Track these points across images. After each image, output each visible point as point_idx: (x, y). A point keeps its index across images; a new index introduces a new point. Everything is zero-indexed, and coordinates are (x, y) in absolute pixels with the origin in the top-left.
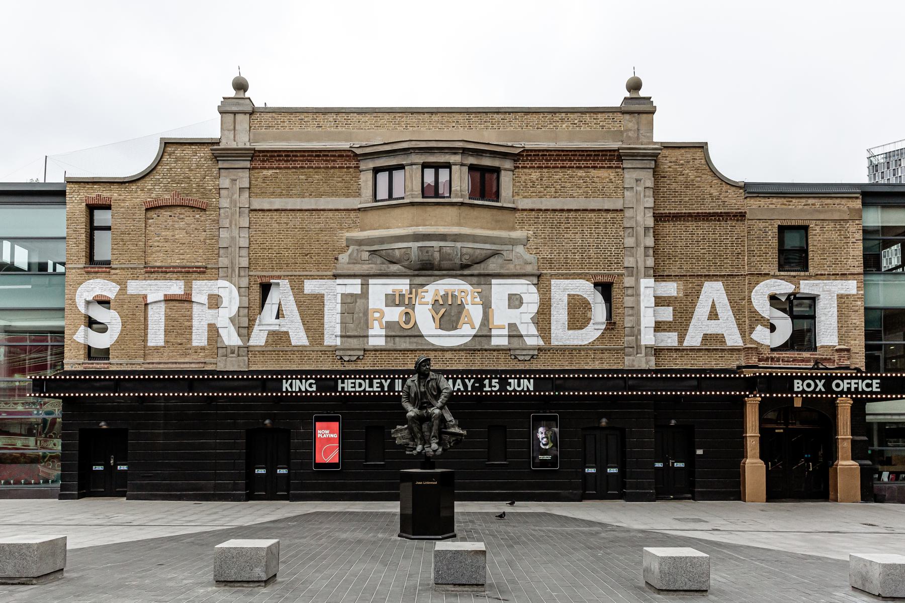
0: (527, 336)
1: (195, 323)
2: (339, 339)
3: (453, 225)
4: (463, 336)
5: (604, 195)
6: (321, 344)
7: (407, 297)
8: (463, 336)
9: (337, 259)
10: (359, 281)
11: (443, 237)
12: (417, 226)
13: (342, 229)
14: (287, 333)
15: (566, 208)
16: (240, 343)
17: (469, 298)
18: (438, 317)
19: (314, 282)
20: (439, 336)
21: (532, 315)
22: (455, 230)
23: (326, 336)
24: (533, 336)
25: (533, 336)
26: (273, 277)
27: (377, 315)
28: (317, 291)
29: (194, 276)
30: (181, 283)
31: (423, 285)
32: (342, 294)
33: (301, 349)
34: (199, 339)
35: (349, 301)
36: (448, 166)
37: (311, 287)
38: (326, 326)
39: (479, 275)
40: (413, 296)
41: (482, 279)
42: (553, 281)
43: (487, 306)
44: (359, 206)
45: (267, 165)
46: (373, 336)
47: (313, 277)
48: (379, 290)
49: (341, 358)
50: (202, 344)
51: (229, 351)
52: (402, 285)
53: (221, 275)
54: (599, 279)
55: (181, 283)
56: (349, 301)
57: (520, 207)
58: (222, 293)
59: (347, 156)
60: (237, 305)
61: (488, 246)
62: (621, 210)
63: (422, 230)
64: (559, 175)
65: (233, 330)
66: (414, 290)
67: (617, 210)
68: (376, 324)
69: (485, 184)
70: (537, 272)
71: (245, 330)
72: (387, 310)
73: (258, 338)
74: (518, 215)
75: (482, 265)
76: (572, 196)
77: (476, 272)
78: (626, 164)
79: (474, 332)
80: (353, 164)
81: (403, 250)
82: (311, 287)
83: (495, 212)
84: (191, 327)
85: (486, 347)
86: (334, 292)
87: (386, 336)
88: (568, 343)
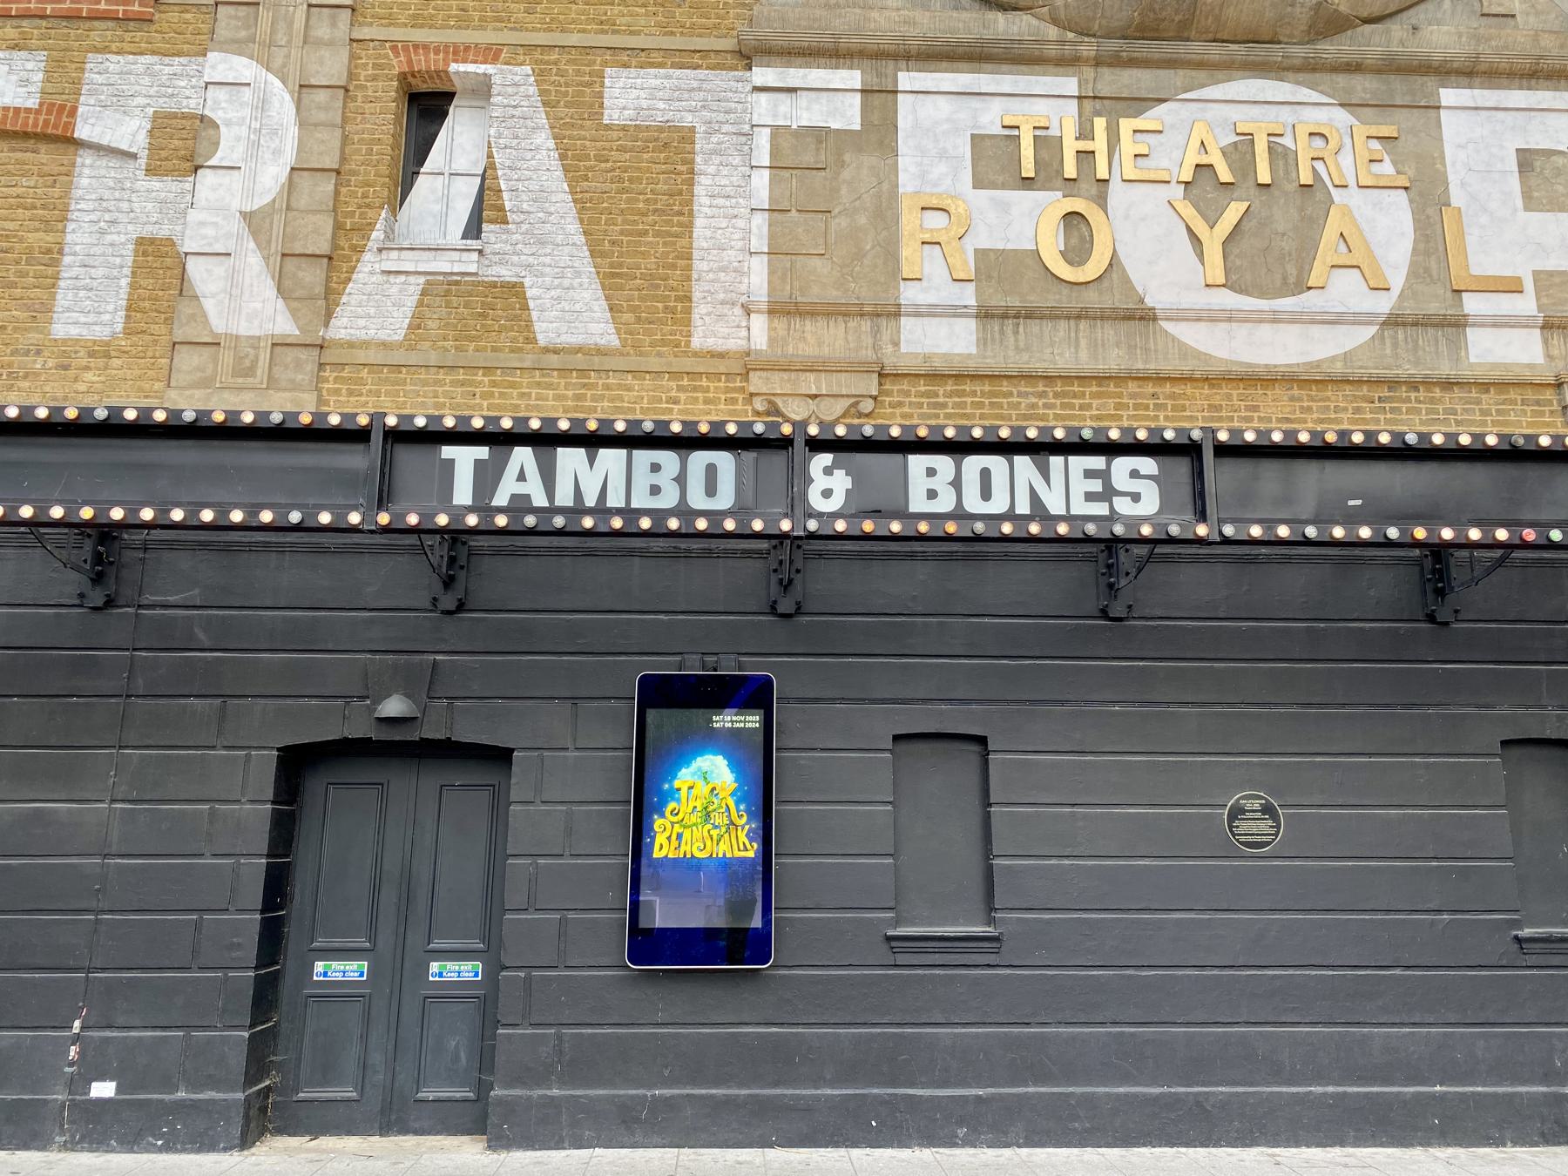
1: (78, 237)
2: (759, 323)
4: (1337, 320)
6: (680, 346)
7: (1070, 147)
8: (1337, 320)
10: (852, 77)
14: (515, 290)
16: (284, 325)
17: (1346, 160)
18: (1213, 242)
19: (653, 78)
20: (1230, 317)
23: (700, 310)
26: (462, 52)
27: (936, 221)
28: (662, 113)
29: (100, 32)
30: (33, 66)
31: (1138, 103)
32: (777, 132)
33: (579, 360)
34: (89, 303)
35: (808, 159)
37: (630, 95)
38: (699, 266)
39: (1393, 67)
40: (1100, 144)
41: (1399, 88)
43: (1428, 195)
46: (918, 313)
47: (642, 58)
48: (940, 116)
50: (101, 333)
51: (226, 357)
52: (1044, 104)
53: (222, 32)
55: (33, 66)
56: (804, 158)
58: (220, 107)
60: (289, 157)
65: (253, 262)
66: (1100, 123)
68: (933, 266)
71: (318, 268)
73: (376, 308)
79: (1383, 304)
82: (630, 95)
84: (53, 256)
85: (1445, 369)
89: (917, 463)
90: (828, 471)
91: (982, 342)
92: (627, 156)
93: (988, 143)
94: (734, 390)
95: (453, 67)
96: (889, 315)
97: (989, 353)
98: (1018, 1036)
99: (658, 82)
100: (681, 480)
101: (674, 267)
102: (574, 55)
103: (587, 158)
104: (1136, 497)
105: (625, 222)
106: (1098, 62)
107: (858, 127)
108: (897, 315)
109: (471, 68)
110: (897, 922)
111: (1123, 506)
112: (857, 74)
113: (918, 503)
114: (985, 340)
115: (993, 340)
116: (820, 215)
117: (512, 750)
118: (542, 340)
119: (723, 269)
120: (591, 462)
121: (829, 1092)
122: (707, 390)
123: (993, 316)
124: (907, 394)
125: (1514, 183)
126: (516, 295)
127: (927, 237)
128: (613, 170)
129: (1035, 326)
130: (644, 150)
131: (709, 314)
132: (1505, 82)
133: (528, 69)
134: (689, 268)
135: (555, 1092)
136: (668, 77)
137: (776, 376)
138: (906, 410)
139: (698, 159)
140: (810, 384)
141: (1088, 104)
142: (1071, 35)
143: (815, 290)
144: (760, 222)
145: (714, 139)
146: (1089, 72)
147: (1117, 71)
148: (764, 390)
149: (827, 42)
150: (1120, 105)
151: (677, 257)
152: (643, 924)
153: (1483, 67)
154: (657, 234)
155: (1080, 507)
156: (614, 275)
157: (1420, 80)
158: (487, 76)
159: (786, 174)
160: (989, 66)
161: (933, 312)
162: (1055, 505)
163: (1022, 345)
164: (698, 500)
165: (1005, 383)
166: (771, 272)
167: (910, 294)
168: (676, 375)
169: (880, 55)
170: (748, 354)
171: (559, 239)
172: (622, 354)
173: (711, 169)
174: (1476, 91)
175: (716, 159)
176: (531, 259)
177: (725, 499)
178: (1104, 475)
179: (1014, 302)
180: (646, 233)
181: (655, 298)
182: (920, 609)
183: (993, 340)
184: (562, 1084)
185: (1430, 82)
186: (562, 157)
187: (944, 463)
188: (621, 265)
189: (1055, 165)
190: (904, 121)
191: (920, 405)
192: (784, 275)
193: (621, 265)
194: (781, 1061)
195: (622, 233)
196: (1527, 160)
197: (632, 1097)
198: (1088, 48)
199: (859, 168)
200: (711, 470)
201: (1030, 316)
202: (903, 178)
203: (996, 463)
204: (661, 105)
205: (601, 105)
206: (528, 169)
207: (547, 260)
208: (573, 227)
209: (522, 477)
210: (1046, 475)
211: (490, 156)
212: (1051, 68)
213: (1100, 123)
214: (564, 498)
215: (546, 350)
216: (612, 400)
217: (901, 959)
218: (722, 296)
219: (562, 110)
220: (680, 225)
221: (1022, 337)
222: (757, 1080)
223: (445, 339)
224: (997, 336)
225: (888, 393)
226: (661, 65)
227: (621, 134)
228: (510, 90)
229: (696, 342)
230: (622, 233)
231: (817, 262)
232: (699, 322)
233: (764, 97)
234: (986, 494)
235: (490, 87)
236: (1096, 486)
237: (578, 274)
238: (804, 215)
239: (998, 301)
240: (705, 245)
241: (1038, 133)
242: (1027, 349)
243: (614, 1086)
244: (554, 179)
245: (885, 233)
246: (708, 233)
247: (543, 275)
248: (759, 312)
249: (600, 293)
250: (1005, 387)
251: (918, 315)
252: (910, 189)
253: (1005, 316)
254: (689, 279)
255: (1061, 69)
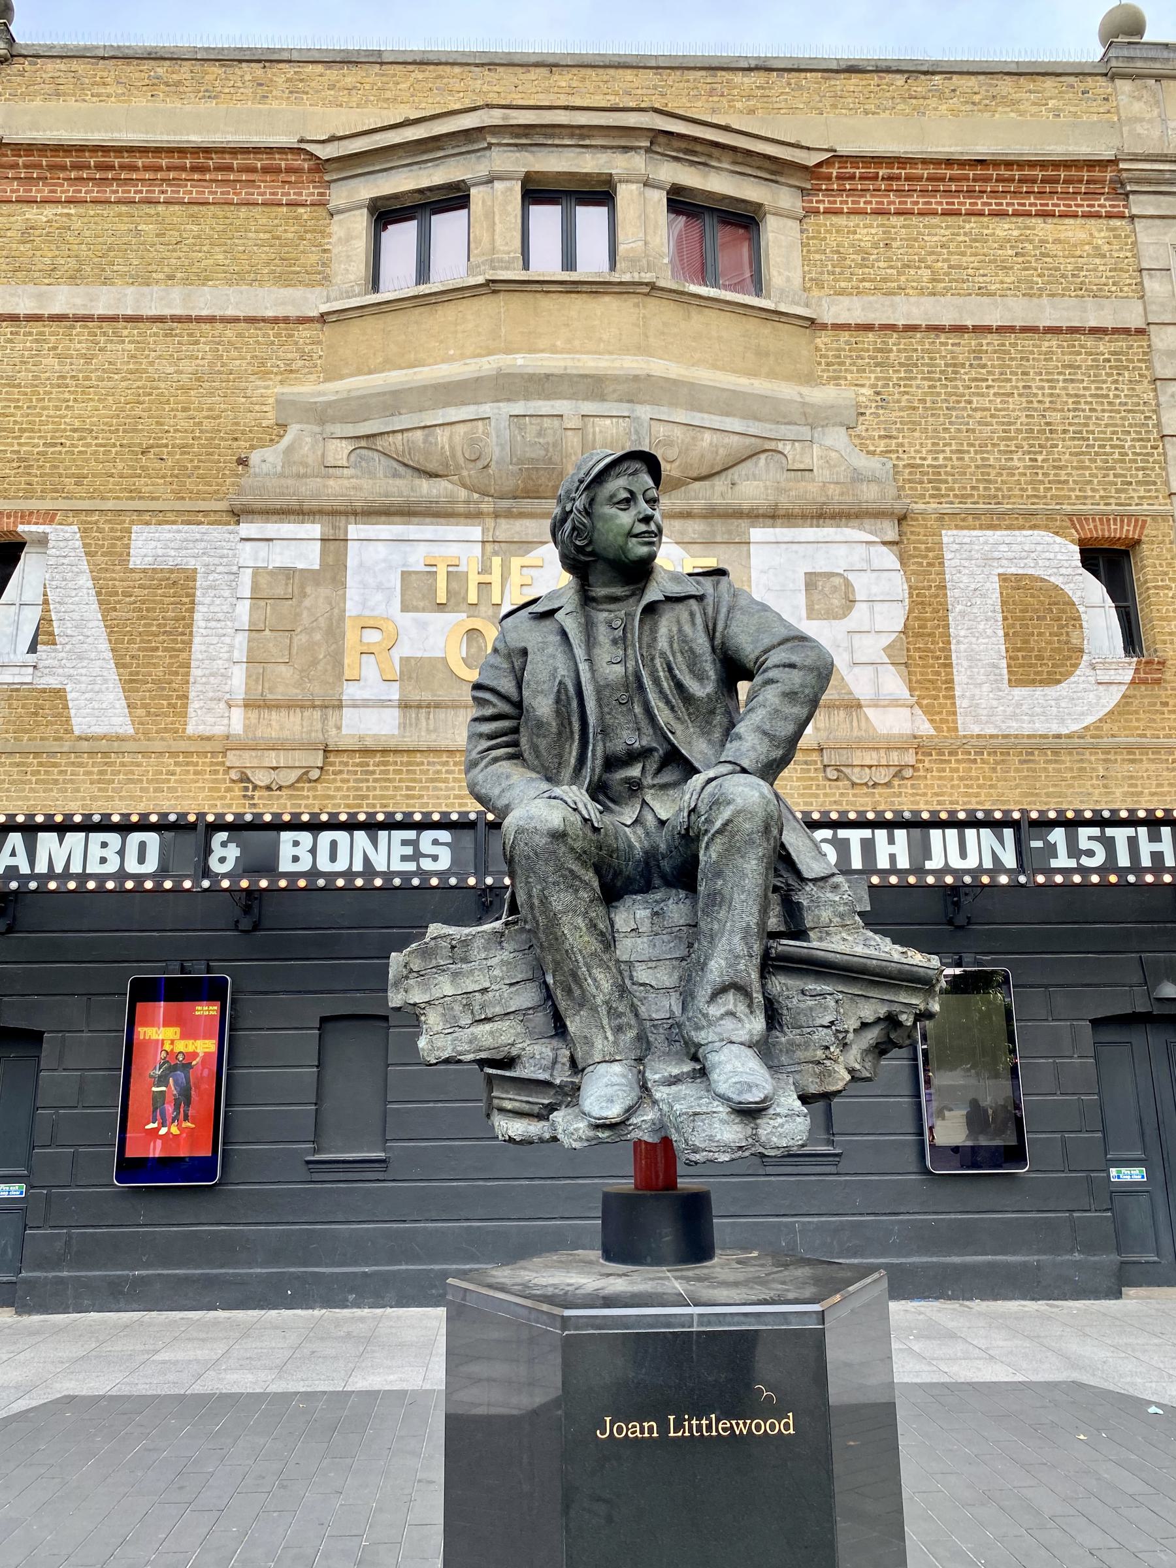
0: (876, 704)
2: (237, 714)
3: (626, 350)
5: (1082, 290)
6: (177, 733)
7: (474, 580)
9: (243, 462)
10: (314, 530)
11: (593, 386)
12: (508, 351)
13: (265, 374)
15: (969, 323)
19: (167, 532)
21: (887, 640)
22: (632, 364)
23: (194, 705)
24: (895, 703)
25: (895, 703)
26: (26, 516)
27: (372, 637)
32: (257, 571)
35: (279, 591)
36: (600, 193)
37: (149, 546)
38: (194, 672)
39: (712, 514)
40: (495, 578)
42: (948, 536)
44: (324, 308)
45: (40, 191)
47: (160, 517)
49: (245, 779)
54: (1095, 531)
56: (279, 592)
57: (828, 319)
59: (290, 170)
61: (734, 424)
62: (1140, 332)
63: (521, 362)
64: (938, 231)
66: (496, 561)
67: (1126, 331)
68: (370, 669)
69: (719, 225)
70: (899, 507)
72: (406, 620)
74: (823, 339)
75: (720, 484)
76: (983, 292)
77: (698, 504)
78: (1139, 205)
80: (309, 193)
81: (461, 429)
82: (149, 546)
83: (752, 325)
86: (231, 565)
87: (405, 705)
88: (1013, 727)
89: (286, 837)
90: (224, 844)
91: (403, 726)
92: (146, 592)
93: (414, 577)
94: (217, 764)
95: (21, 528)
96: (334, 707)
97: (407, 734)
98: (397, 1230)
99: (170, 535)
100: (121, 853)
101: (177, 673)
102: (110, 516)
103: (116, 594)
104: (435, 858)
105: (142, 641)
106: (496, 515)
107: (318, 567)
108: (340, 707)
109: (33, 528)
110: (315, 1151)
111: (427, 865)
112: (318, 527)
113: (285, 866)
114: (405, 724)
115: (411, 725)
116: (287, 634)
117: (44, 1032)
118: (77, 733)
119: (212, 675)
120: (61, 841)
121: (259, 1270)
122: (197, 764)
123: (411, 707)
124: (346, 764)
125: (801, 599)
126: (60, 698)
127: (365, 649)
128: (135, 602)
129: (441, 714)
130: (159, 587)
131: (201, 708)
132: (800, 522)
133: (75, 528)
134: (188, 674)
135: (65, 1274)
136: (179, 531)
137: (246, 754)
138: (345, 776)
139: (198, 593)
140: (272, 759)
141: (489, 547)
142: (476, 496)
143: (281, 689)
144: (241, 640)
145: (211, 577)
146: (490, 522)
147: (512, 521)
148: (237, 765)
149: (294, 504)
150: (513, 547)
151: (179, 667)
152: (129, 1154)
153: (782, 512)
154: (165, 650)
155: (397, 866)
156: (132, 681)
157: (736, 522)
158: (46, 534)
159: (262, 603)
160: (416, 520)
161: (365, 704)
162: (380, 865)
163: (431, 727)
164: (132, 867)
165: (418, 755)
166: (248, 676)
167: (351, 692)
168: (173, 754)
169: (334, 513)
170: (228, 737)
171: (93, 656)
172: (135, 740)
173: (207, 600)
174: (777, 530)
175: (212, 593)
176: (71, 671)
177: (151, 866)
178: (415, 843)
179: (427, 696)
180: (156, 649)
181: (161, 697)
182: (346, 924)
183: (411, 725)
184: (70, 1268)
185: (744, 523)
186: (98, 594)
187: (305, 837)
188: (137, 673)
189: (463, 592)
190: (352, 562)
191: (356, 773)
192: (258, 679)
193: (137, 673)
194: (228, 1249)
195: (139, 649)
196: (812, 581)
197: (119, 1276)
198: (487, 506)
199: (317, 598)
200: (142, 846)
201: (437, 706)
202: (349, 605)
203: (341, 836)
204: (173, 553)
205: (128, 554)
206: (72, 604)
207: (83, 671)
208: (104, 646)
209: (13, 854)
210: (375, 842)
211: (45, 595)
212: (462, 520)
213: (496, 561)
214: (41, 868)
215: (80, 738)
216: (126, 774)
217: (316, 1177)
218: (211, 694)
219: (99, 559)
220: (183, 642)
221: (431, 722)
222: (211, 1263)
223: (7, 732)
224: (413, 721)
225: (332, 764)
226: (174, 523)
227: (142, 575)
228: (62, 544)
229: (190, 730)
230: (139, 649)
231: (283, 668)
232: (193, 714)
233: (248, 544)
234: (333, 858)
235: (47, 542)
236: (409, 850)
237: (106, 681)
238: (274, 634)
239: (415, 696)
240: (200, 657)
241: (450, 569)
242: (435, 730)
243: (104, 1267)
244: (92, 610)
245: (334, 646)
246: (203, 648)
247: (80, 682)
248: (237, 706)
249: (121, 695)
250: (419, 758)
251: (355, 706)
252: (353, 613)
253: (419, 707)
254: (188, 682)
255: (469, 521)
